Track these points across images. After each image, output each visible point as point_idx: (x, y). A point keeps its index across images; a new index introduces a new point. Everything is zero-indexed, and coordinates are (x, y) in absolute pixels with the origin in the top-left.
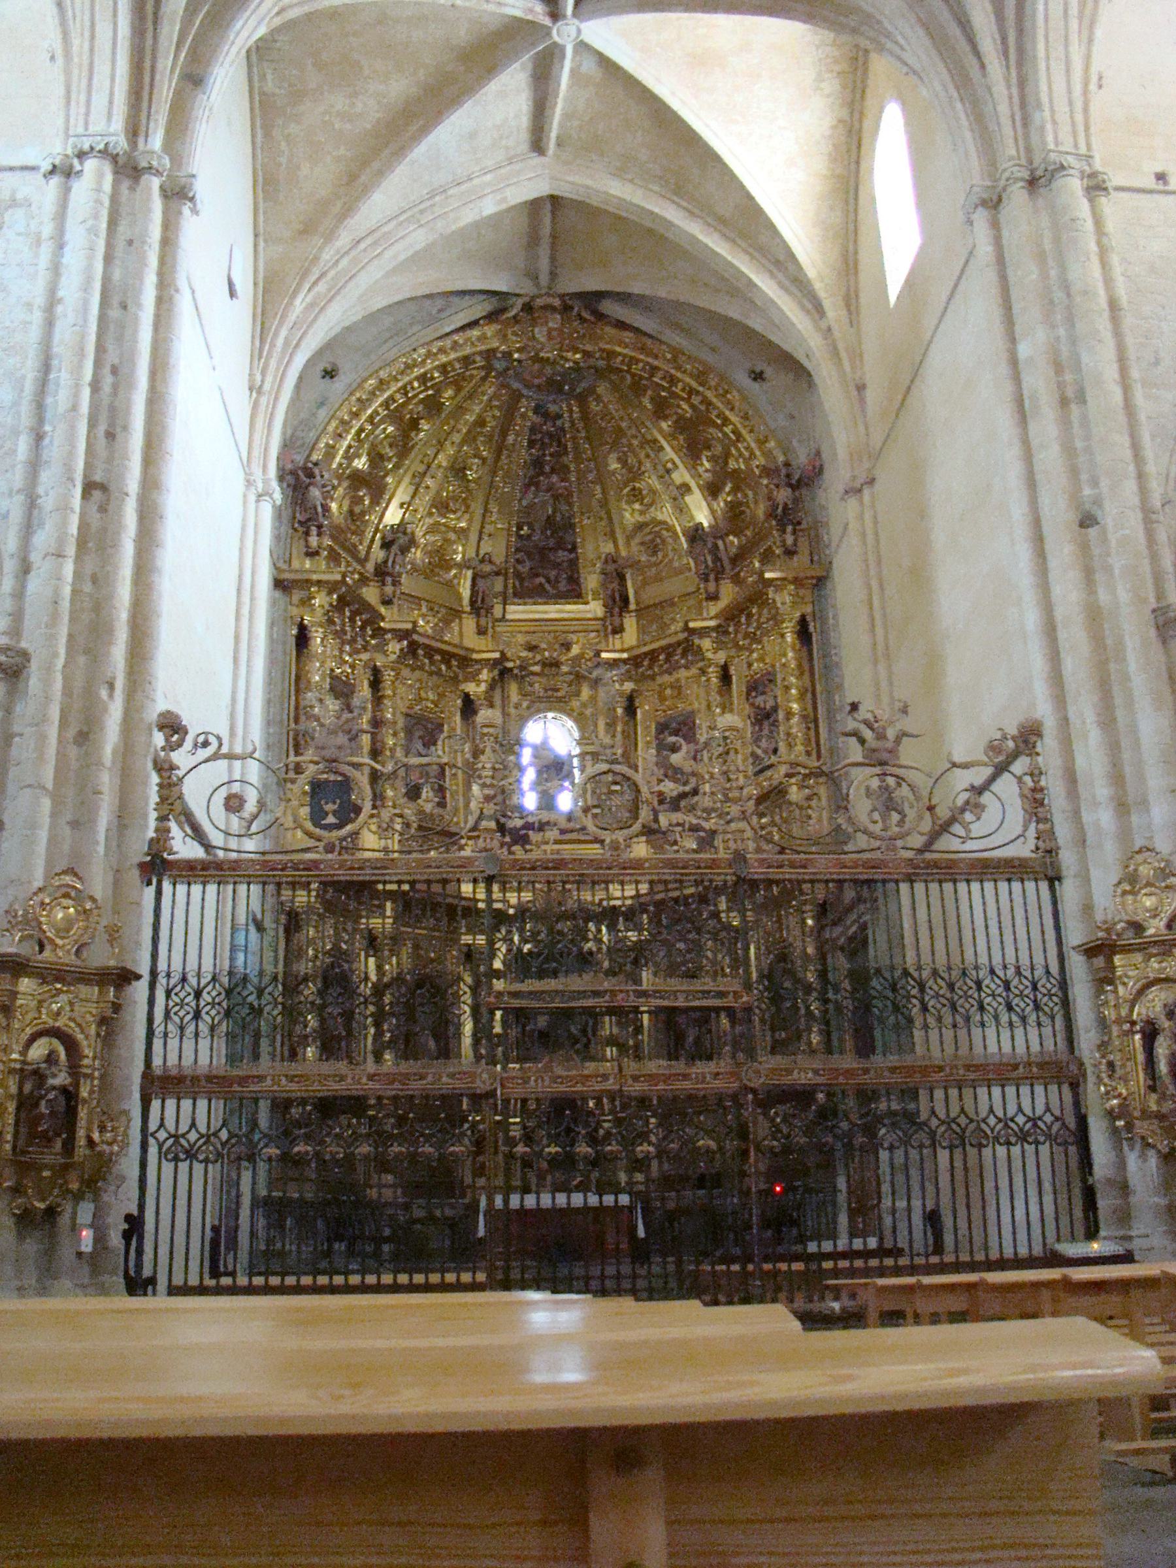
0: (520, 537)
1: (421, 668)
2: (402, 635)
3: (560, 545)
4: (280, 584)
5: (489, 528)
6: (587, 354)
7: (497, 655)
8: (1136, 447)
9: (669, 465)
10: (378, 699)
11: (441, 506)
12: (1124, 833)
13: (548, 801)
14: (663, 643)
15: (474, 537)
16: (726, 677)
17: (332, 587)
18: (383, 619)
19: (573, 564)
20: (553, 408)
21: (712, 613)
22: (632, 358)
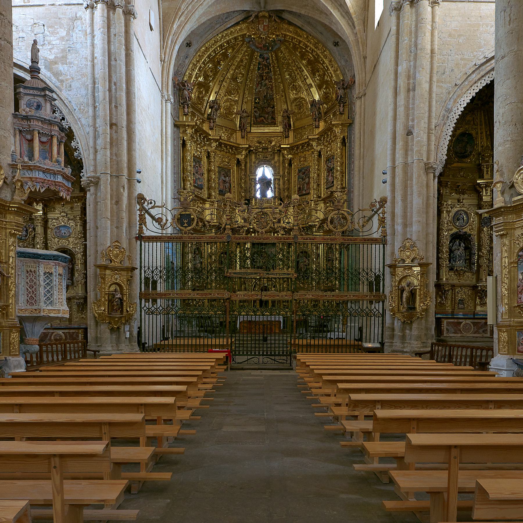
0: (256, 103)
1: (223, 151)
2: (216, 140)
3: (269, 105)
4: (176, 126)
5: (245, 100)
6: (277, 36)
7: (247, 146)
8: (430, 106)
9: (305, 77)
10: (209, 163)
11: (229, 92)
12: (405, 233)
13: (264, 194)
14: (301, 142)
15: (240, 102)
16: (320, 155)
17: (192, 127)
18: (210, 135)
19: (273, 112)
20: (266, 56)
21: (317, 133)
22: (292, 37)
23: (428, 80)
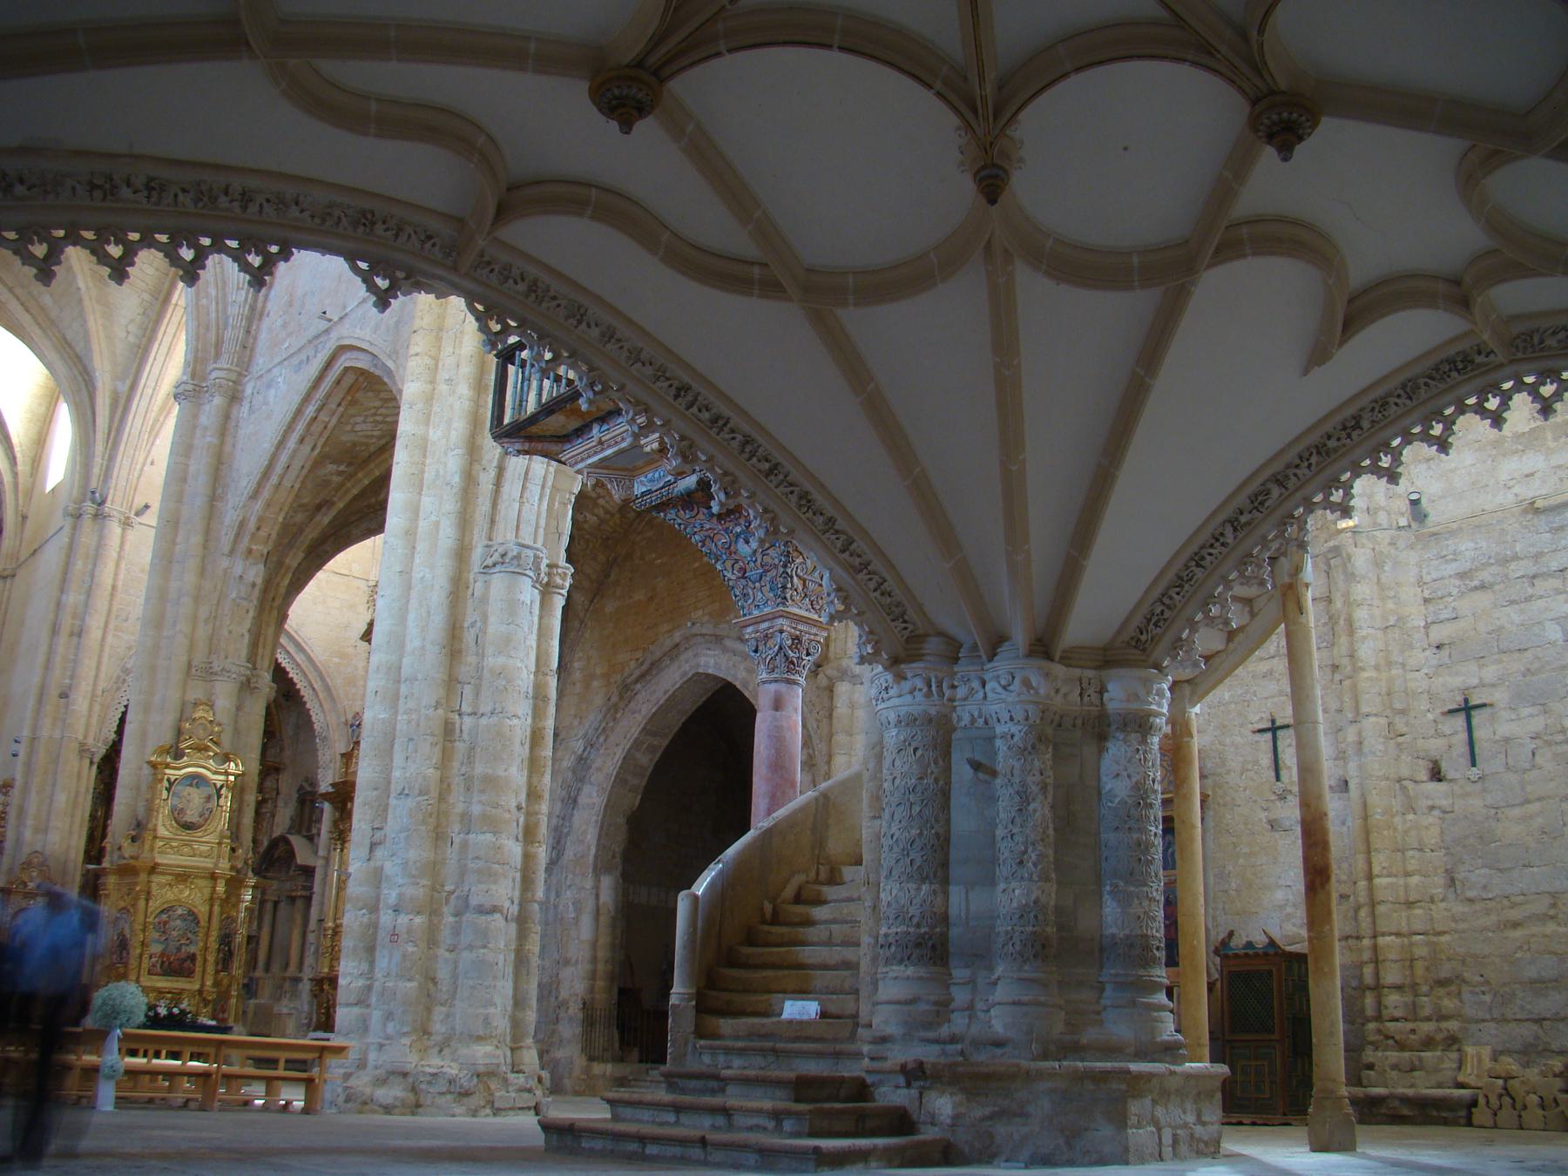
23: (102, 625)
